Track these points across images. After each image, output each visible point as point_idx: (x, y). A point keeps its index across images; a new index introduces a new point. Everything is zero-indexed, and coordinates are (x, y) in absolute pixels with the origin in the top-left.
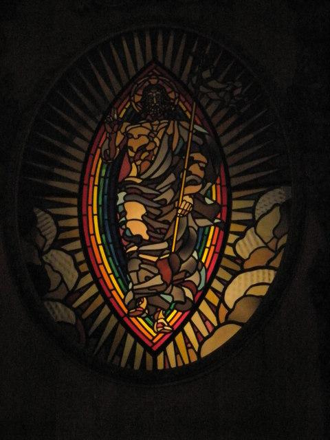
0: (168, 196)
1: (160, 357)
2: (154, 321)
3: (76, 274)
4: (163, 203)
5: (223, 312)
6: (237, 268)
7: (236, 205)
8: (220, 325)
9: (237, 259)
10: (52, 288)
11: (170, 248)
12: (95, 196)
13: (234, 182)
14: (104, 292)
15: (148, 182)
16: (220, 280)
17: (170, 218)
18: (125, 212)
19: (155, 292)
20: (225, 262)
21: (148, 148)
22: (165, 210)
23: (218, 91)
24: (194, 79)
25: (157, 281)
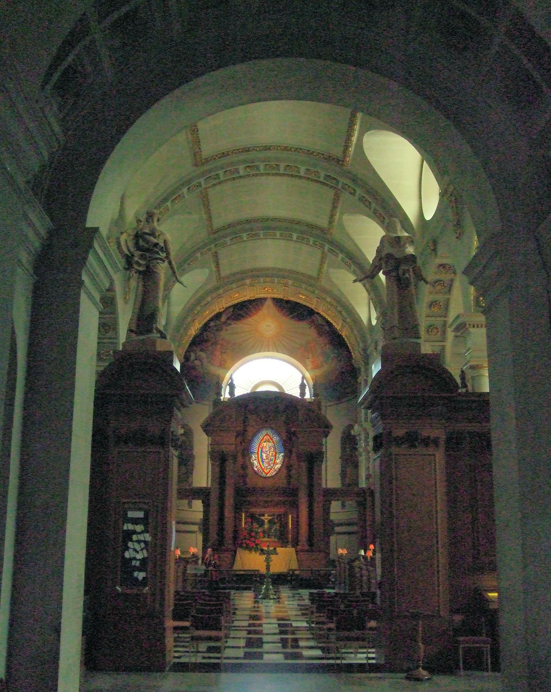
14: (261, 466)
19: (267, 467)
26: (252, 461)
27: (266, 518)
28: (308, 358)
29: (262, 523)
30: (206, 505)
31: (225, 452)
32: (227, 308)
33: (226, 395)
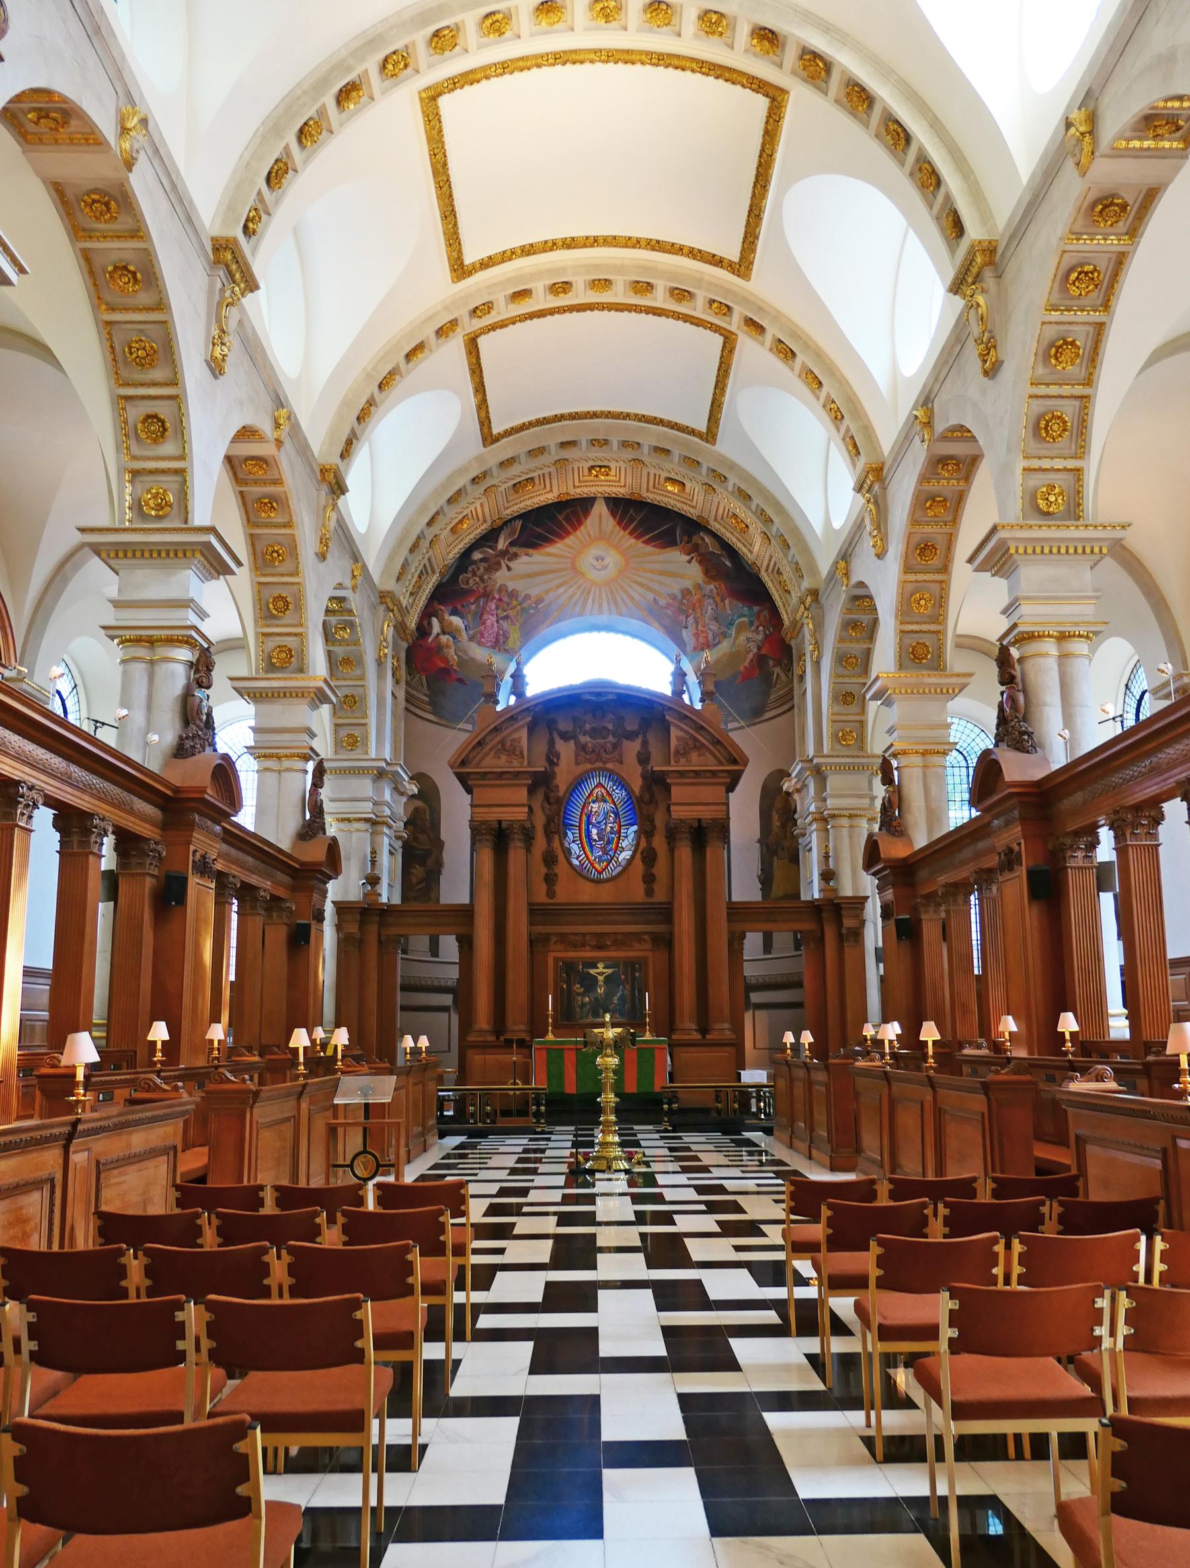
14: (587, 856)
19: (600, 857)
27: (601, 971)
28: (686, 627)
29: (590, 983)
30: (466, 944)
31: (504, 825)
32: (507, 523)
33: (506, 700)
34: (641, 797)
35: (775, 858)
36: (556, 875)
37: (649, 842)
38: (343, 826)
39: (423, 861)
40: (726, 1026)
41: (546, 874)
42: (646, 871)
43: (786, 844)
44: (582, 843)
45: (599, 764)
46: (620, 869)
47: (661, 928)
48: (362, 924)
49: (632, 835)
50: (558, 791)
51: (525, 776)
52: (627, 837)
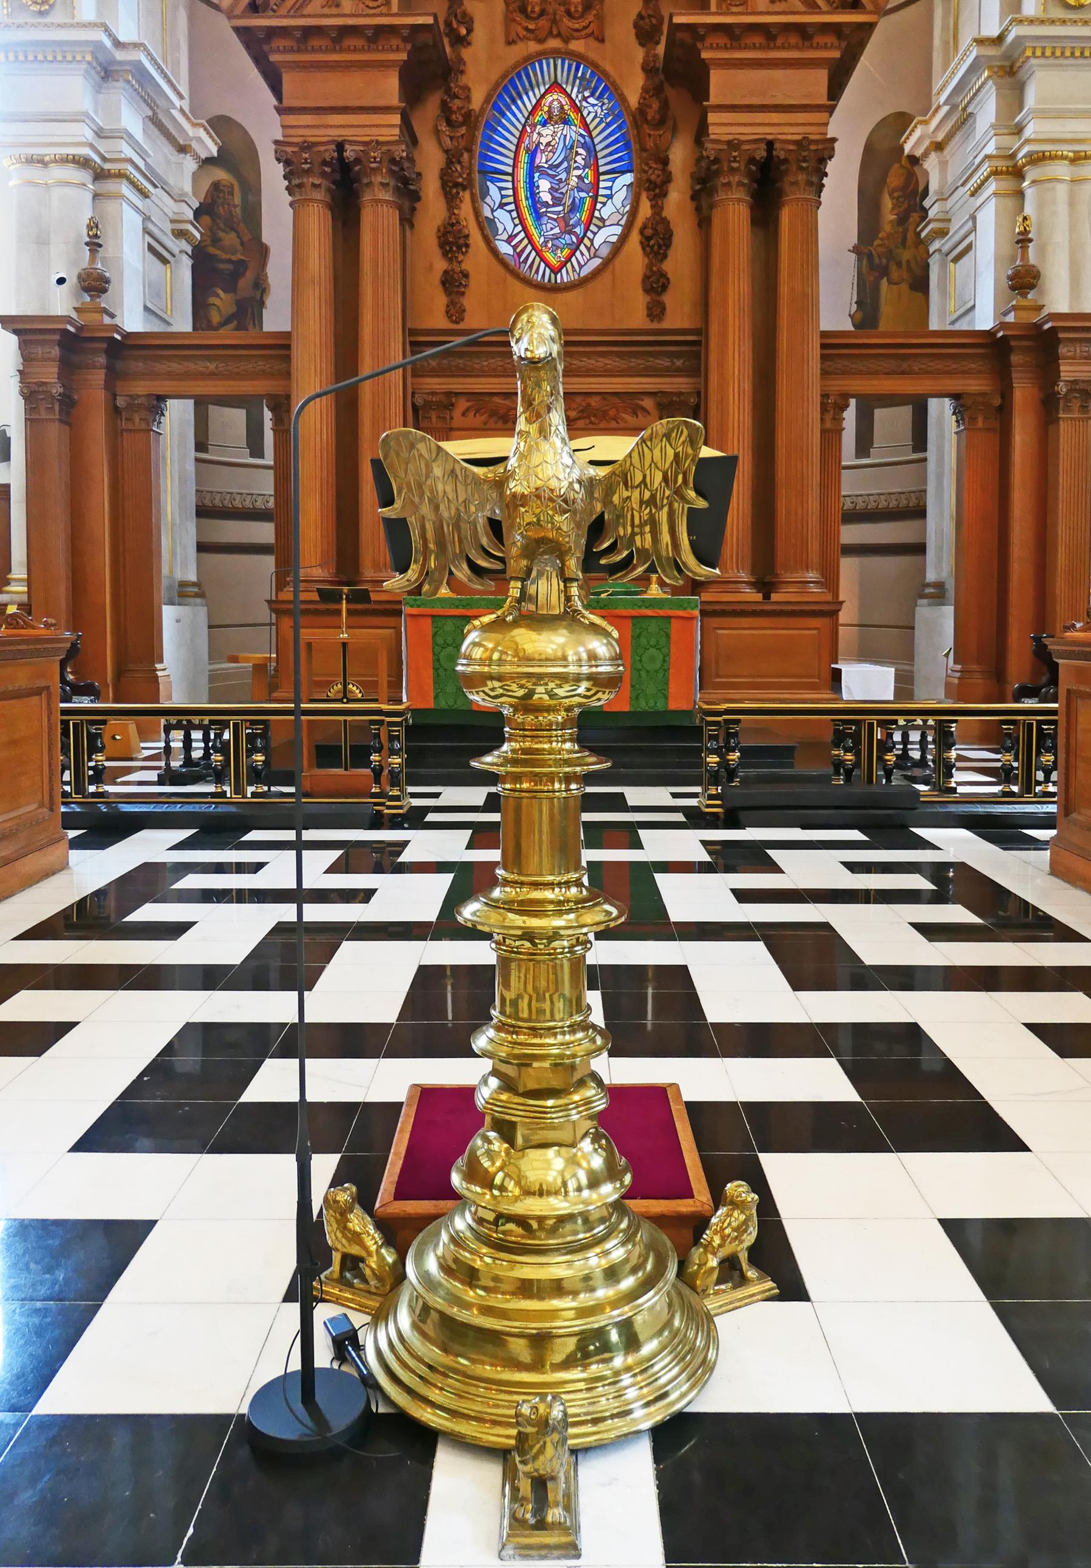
0: (563, 176)
1: (559, 276)
2: (556, 255)
3: (513, 226)
4: (560, 181)
5: (593, 250)
6: (601, 224)
7: (602, 184)
8: (591, 259)
9: (602, 220)
10: (500, 233)
11: (564, 209)
12: (522, 174)
13: (602, 169)
14: (528, 236)
15: (552, 167)
16: (592, 231)
17: (563, 191)
18: (538, 187)
19: (556, 237)
20: (595, 221)
21: (552, 144)
22: (562, 185)
23: (593, 105)
24: (580, 96)
25: (557, 230)
26: (487, 213)
31: (349, 153)
34: (642, 110)
35: (885, 281)
36: (466, 275)
37: (657, 208)
38: (36, 173)
39: (230, 283)
40: (812, 575)
41: (446, 272)
42: (649, 267)
43: (906, 255)
44: (518, 208)
45: (554, 43)
46: (597, 262)
47: (679, 384)
48: (68, 368)
49: (623, 193)
50: (468, 99)
51: (395, 42)
52: (610, 197)
